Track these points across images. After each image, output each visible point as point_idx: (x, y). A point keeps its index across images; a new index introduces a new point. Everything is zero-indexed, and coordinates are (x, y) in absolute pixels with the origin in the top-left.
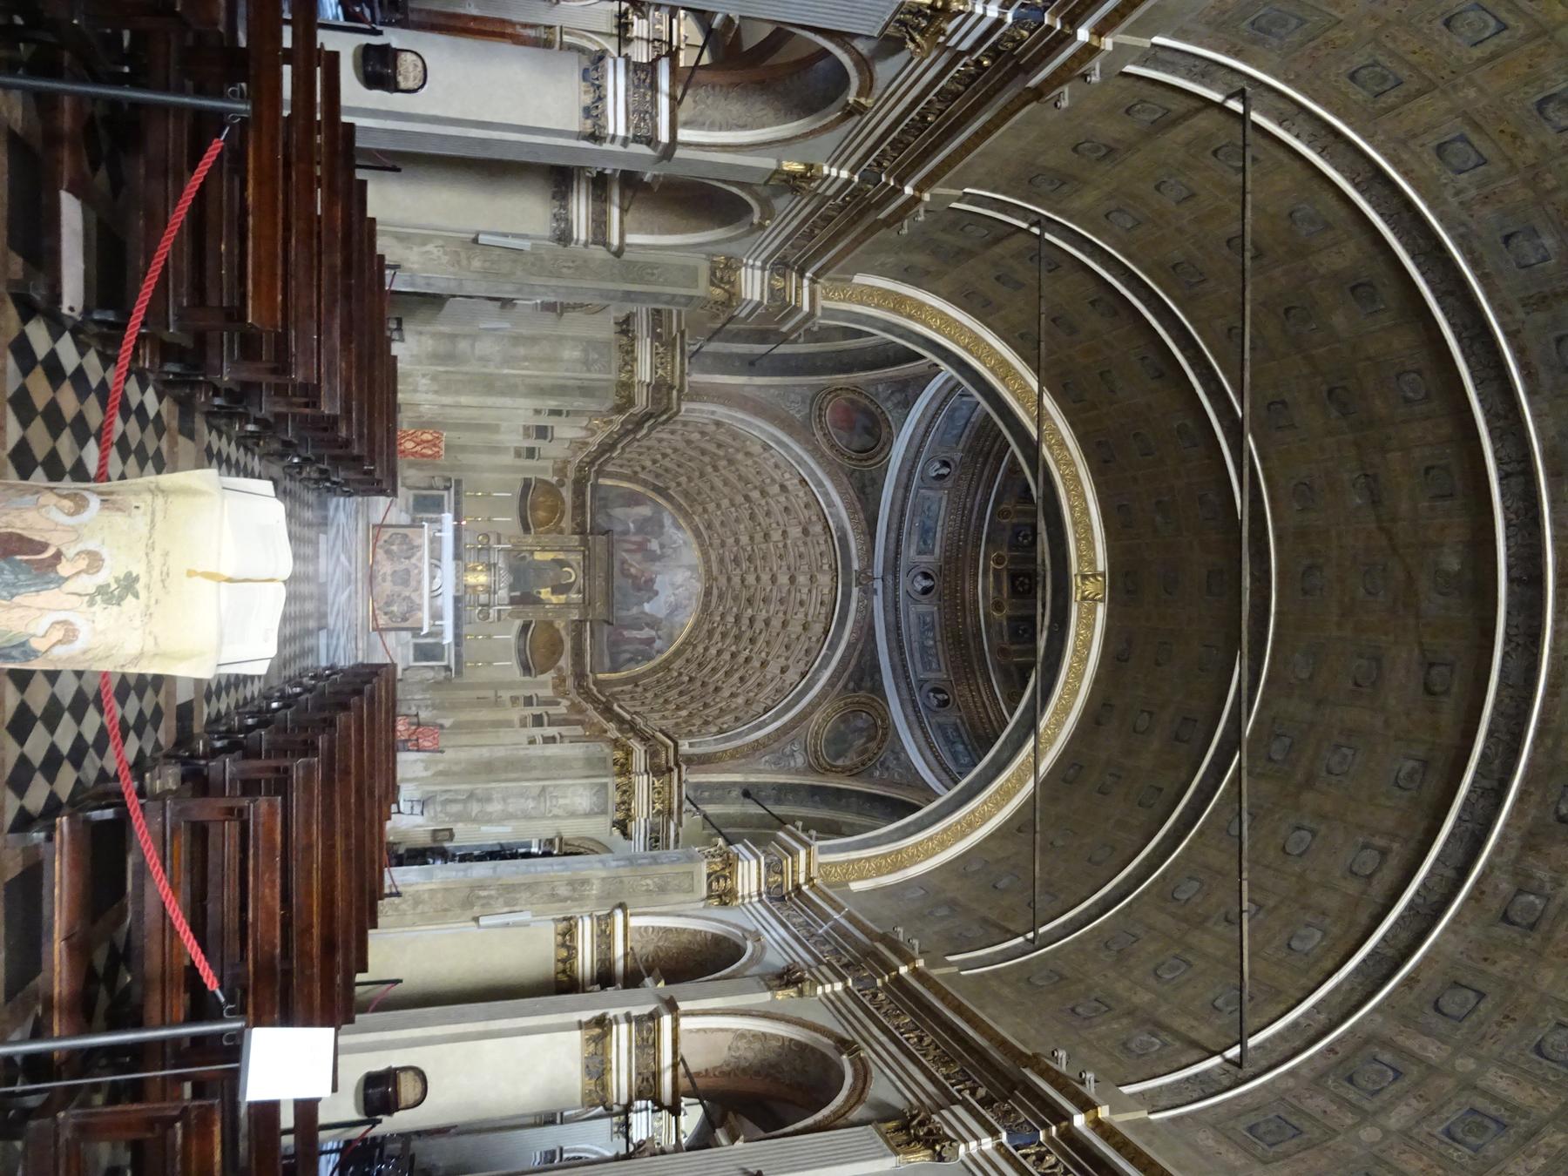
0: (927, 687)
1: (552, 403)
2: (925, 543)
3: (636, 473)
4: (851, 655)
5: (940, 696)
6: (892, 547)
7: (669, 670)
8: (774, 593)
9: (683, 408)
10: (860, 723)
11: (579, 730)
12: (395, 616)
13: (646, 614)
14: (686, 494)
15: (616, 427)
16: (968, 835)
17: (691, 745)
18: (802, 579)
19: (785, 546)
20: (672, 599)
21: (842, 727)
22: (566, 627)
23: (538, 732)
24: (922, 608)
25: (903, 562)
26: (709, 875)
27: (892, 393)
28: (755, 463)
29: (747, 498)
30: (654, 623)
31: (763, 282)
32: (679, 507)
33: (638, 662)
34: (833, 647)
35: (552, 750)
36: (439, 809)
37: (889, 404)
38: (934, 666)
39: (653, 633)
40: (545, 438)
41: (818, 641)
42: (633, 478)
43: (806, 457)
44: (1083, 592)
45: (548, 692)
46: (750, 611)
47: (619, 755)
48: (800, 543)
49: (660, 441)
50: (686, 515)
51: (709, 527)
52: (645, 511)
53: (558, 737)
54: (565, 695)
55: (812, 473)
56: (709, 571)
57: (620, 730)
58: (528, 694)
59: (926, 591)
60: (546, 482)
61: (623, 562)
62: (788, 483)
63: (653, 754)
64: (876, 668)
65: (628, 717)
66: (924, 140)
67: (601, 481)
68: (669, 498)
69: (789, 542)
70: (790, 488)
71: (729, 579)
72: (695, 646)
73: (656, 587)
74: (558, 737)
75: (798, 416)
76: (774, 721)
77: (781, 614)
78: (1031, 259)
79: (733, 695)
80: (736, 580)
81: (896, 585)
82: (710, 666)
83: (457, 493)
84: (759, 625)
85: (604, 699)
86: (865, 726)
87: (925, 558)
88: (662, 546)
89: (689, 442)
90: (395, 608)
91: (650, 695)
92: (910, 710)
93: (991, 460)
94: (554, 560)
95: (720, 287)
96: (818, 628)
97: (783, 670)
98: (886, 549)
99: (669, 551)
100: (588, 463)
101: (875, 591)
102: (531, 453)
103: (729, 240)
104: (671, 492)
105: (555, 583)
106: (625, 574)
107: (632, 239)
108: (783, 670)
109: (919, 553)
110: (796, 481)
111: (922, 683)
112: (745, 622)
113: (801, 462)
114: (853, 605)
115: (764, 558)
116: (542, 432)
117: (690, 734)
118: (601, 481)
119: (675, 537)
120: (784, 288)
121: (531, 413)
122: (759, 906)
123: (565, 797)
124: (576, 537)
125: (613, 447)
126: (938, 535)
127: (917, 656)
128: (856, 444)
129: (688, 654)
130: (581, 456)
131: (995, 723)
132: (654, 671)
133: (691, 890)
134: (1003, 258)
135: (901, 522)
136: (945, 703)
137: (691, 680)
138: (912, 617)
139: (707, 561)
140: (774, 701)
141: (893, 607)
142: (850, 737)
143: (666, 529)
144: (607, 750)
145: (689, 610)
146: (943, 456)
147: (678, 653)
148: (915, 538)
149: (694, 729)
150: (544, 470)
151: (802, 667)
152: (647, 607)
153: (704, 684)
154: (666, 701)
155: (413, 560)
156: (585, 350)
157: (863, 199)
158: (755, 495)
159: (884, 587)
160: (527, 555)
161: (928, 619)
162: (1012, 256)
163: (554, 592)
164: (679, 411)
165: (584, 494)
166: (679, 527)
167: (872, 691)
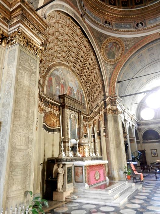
7: (86, 92)
10: (109, 47)
17: (107, 92)
19: (69, 37)
21: (107, 52)
30: (78, 92)
52: (54, 80)
57: (102, 110)
64: (101, 34)
65: (98, 108)
72: (82, 82)
73: (71, 87)
74: (104, 128)
84: (82, 59)
85: (93, 113)
86: (111, 45)
88: (62, 79)
92: (114, 32)
97: (92, 60)
131: (119, 14)
142: (111, 51)
143: (58, 75)
144: (110, 115)
152: (75, 92)
156: (25, 69)
167: (105, 38)
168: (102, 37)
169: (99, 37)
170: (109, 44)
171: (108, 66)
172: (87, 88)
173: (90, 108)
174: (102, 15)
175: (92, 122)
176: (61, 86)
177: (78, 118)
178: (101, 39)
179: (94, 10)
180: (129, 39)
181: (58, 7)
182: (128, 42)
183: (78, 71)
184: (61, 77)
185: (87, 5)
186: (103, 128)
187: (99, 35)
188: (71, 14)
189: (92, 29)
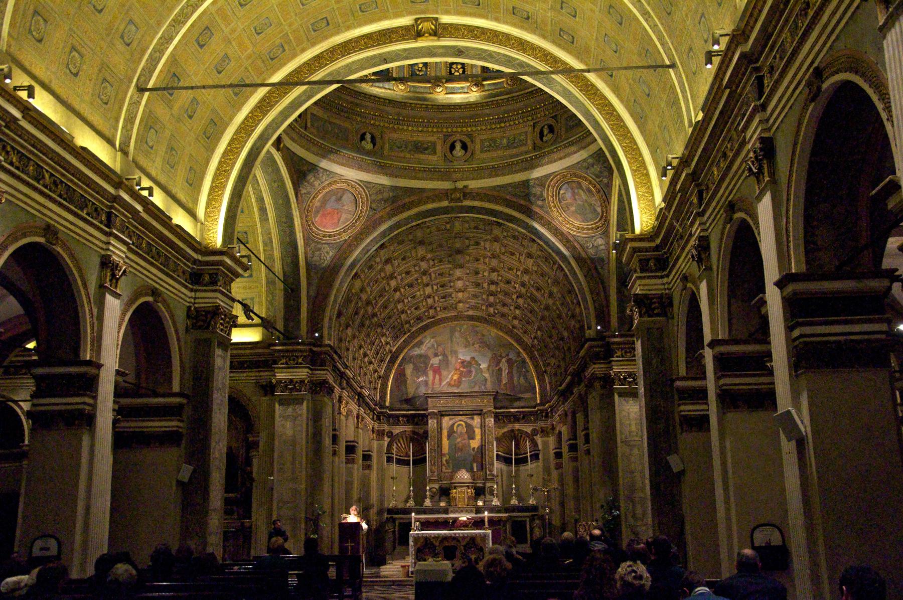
0: (538, 142)
1: (327, 441)
2: (426, 149)
3: (380, 377)
5: (546, 131)
7: (533, 346)
9: (327, 342)
11: (580, 417)
12: (478, 557)
13: (489, 366)
14: (396, 338)
15: (345, 394)
16: (619, 116)
18: (458, 245)
20: (477, 346)
21: (573, 209)
22: (500, 427)
23: (582, 447)
24: (478, 147)
25: (442, 165)
26: (649, 316)
27: (308, 182)
28: (369, 284)
29: (395, 290)
31: (205, 291)
32: (406, 343)
33: (527, 371)
34: (511, 219)
35: (594, 436)
36: (639, 523)
37: (316, 183)
38: (523, 137)
39: (504, 360)
40: (354, 447)
41: (507, 231)
42: (385, 378)
43: (363, 246)
44: (430, 35)
45: (552, 440)
46: (485, 285)
47: (597, 385)
48: (430, 248)
49: (354, 359)
50: (413, 336)
51: (419, 319)
52: (409, 370)
53: (584, 433)
54: (553, 428)
56: (455, 318)
57: (579, 384)
58: (552, 456)
59: (464, 147)
60: (390, 445)
61: (449, 384)
63: (595, 358)
65: (569, 378)
66: (75, 184)
67: (387, 404)
68: (400, 350)
70: (387, 256)
71: (460, 302)
72: (514, 327)
74: (584, 433)
75: (331, 254)
78: (171, 95)
79: (551, 295)
80: (460, 295)
81: (459, 170)
82: (529, 315)
83: (397, 513)
84: (494, 276)
87: (439, 148)
88: (436, 355)
89: (354, 337)
90: (473, 557)
91: (553, 361)
93: (358, 101)
94: (449, 436)
95: (210, 321)
96: (497, 231)
98: (431, 179)
99: (440, 349)
100: (374, 413)
101: (465, 187)
102: (367, 457)
103: (172, 316)
104: (394, 350)
105: (466, 436)
106: (459, 383)
107: (176, 388)
108: (529, 256)
109: (435, 153)
110: (382, 252)
111: (535, 148)
112: (493, 288)
113: (366, 250)
114: (477, 204)
115: (441, 275)
116: (351, 449)
117: (582, 328)
118: (387, 404)
119: (429, 345)
120: (209, 274)
121: (337, 459)
122: (671, 277)
123: (630, 425)
124: (430, 421)
125: (360, 395)
126: (420, 139)
127: (515, 151)
128: (350, 207)
129: (519, 332)
130: (368, 420)
132: (533, 358)
133: (660, 330)
134: (172, 114)
135: (410, 168)
136: (551, 129)
137: (539, 329)
138: (484, 156)
139: (448, 319)
140: (554, 264)
141: (479, 173)
144: (594, 394)
145: (485, 332)
146: (357, 138)
147: (519, 341)
148: (422, 157)
149: (577, 326)
150: (380, 447)
151: (525, 243)
153: (543, 318)
154: (557, 348)
155: (437, 544)
157: (129, 222)
158: (393, 283)
159: (462, 180)
160: (445, 459)
161: (487, 144)
162: (171, 109)
163: (473, 438)
164: (329, 346)
165: (397, 416)
166: (420, 343)
167: (542, 185)
170: (562, 192)
171: (595, 241)
172: (533, 336)
173: (550, 383)
174: (530, 118)
175: (556, 417)
176: (431, 373)
177: (479, 426)
179: (503, 125)
180: (590, 161)
182: (595, 166)
183: (491, 310)
184: (430, 353)
185: (481, 129)
186: (582, 431)
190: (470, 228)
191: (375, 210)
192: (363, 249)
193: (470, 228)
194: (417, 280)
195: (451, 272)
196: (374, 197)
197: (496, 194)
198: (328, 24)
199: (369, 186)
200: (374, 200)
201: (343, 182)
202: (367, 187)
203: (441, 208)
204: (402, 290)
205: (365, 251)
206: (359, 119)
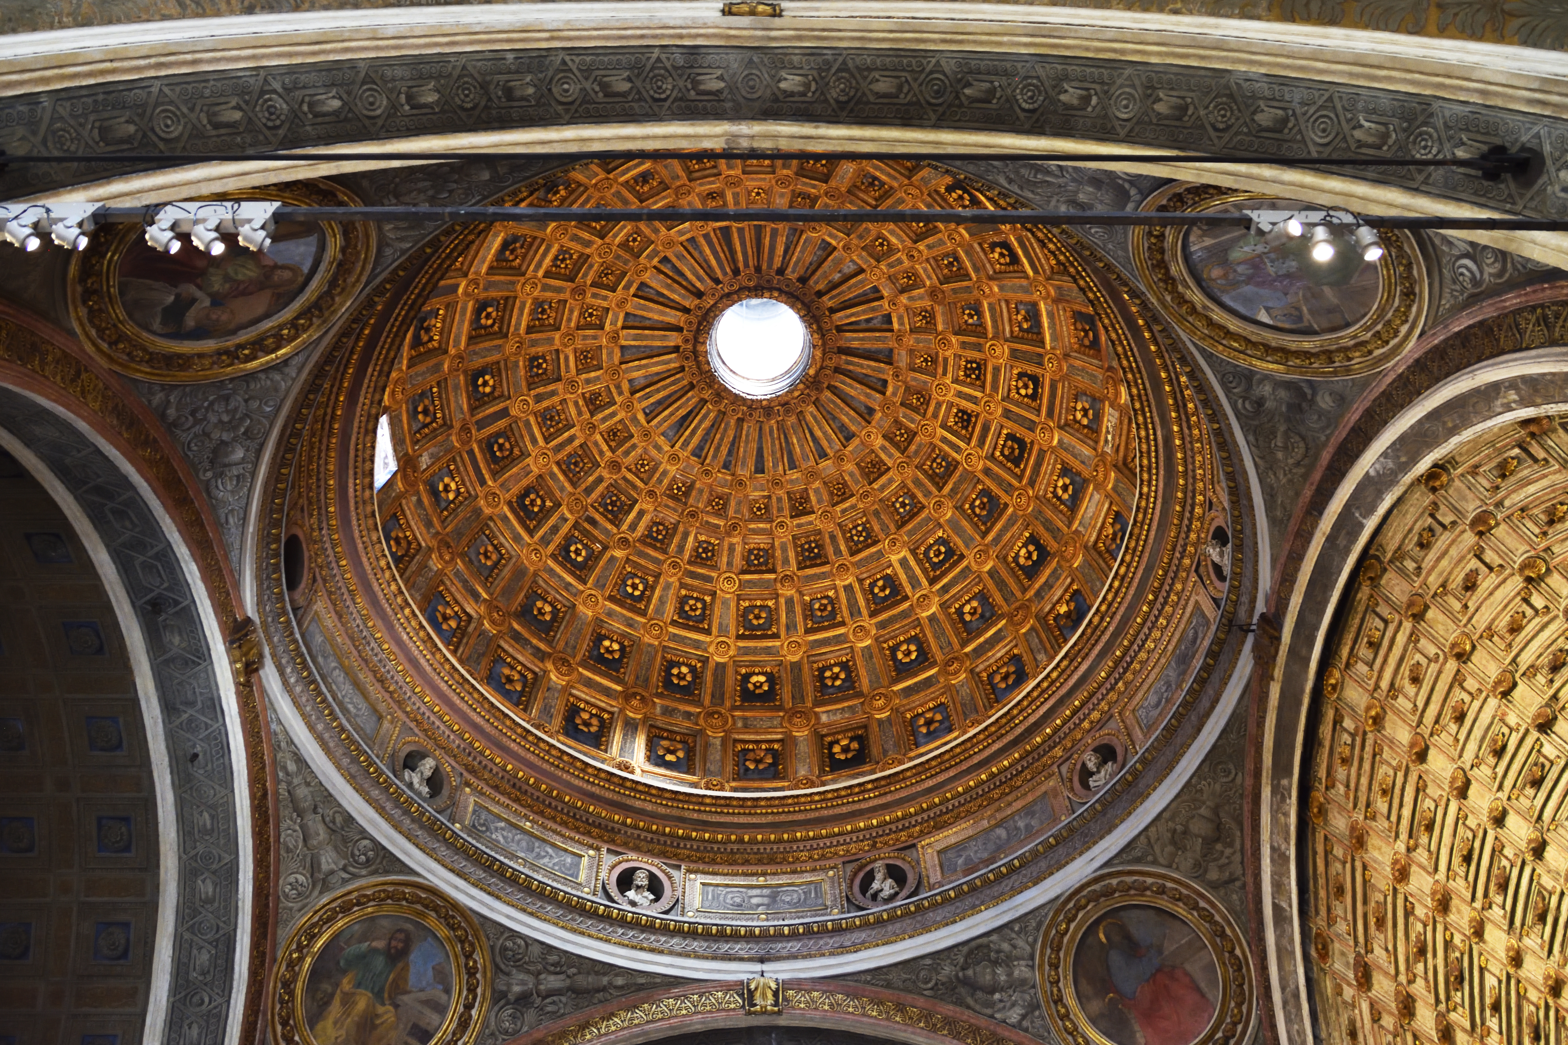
4: (1323, 480)
6: (1215, 678)
8: (1472, 746)
37: (1021, 970)
48: (1382, 824)
55: (1284, 953)
62: (1351, 975)
69: (1401, 846)
76: (1495, 388)
77: (1471, 684)
168: (1269, 404)
169: (1282, 428)
178: (1284, 409)
181: (1293, 987)
187: (1273, 433)
188: (1287, 815)
189: (1279, 513)
190: (1371, 665)
191: (1232, 880)
192: (1285, 1003)
193: (1371, 665)
194: (1448, 944)
195: (1472, 822)
196: (1187, 861)
197: (1292, 526)
198: (126, 820)
199: (1137, 853)
200: (1197, 865)
201: (1078, 908)
202: (1138, 860)
203: (1280, 708)
204: (1453, 1016)
205: (1292, 1001)
206: (1058, 752)
